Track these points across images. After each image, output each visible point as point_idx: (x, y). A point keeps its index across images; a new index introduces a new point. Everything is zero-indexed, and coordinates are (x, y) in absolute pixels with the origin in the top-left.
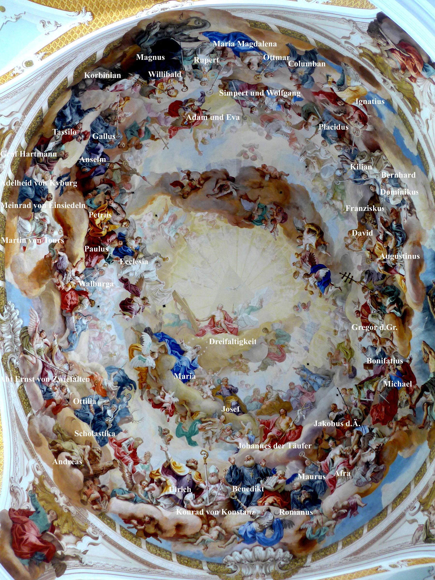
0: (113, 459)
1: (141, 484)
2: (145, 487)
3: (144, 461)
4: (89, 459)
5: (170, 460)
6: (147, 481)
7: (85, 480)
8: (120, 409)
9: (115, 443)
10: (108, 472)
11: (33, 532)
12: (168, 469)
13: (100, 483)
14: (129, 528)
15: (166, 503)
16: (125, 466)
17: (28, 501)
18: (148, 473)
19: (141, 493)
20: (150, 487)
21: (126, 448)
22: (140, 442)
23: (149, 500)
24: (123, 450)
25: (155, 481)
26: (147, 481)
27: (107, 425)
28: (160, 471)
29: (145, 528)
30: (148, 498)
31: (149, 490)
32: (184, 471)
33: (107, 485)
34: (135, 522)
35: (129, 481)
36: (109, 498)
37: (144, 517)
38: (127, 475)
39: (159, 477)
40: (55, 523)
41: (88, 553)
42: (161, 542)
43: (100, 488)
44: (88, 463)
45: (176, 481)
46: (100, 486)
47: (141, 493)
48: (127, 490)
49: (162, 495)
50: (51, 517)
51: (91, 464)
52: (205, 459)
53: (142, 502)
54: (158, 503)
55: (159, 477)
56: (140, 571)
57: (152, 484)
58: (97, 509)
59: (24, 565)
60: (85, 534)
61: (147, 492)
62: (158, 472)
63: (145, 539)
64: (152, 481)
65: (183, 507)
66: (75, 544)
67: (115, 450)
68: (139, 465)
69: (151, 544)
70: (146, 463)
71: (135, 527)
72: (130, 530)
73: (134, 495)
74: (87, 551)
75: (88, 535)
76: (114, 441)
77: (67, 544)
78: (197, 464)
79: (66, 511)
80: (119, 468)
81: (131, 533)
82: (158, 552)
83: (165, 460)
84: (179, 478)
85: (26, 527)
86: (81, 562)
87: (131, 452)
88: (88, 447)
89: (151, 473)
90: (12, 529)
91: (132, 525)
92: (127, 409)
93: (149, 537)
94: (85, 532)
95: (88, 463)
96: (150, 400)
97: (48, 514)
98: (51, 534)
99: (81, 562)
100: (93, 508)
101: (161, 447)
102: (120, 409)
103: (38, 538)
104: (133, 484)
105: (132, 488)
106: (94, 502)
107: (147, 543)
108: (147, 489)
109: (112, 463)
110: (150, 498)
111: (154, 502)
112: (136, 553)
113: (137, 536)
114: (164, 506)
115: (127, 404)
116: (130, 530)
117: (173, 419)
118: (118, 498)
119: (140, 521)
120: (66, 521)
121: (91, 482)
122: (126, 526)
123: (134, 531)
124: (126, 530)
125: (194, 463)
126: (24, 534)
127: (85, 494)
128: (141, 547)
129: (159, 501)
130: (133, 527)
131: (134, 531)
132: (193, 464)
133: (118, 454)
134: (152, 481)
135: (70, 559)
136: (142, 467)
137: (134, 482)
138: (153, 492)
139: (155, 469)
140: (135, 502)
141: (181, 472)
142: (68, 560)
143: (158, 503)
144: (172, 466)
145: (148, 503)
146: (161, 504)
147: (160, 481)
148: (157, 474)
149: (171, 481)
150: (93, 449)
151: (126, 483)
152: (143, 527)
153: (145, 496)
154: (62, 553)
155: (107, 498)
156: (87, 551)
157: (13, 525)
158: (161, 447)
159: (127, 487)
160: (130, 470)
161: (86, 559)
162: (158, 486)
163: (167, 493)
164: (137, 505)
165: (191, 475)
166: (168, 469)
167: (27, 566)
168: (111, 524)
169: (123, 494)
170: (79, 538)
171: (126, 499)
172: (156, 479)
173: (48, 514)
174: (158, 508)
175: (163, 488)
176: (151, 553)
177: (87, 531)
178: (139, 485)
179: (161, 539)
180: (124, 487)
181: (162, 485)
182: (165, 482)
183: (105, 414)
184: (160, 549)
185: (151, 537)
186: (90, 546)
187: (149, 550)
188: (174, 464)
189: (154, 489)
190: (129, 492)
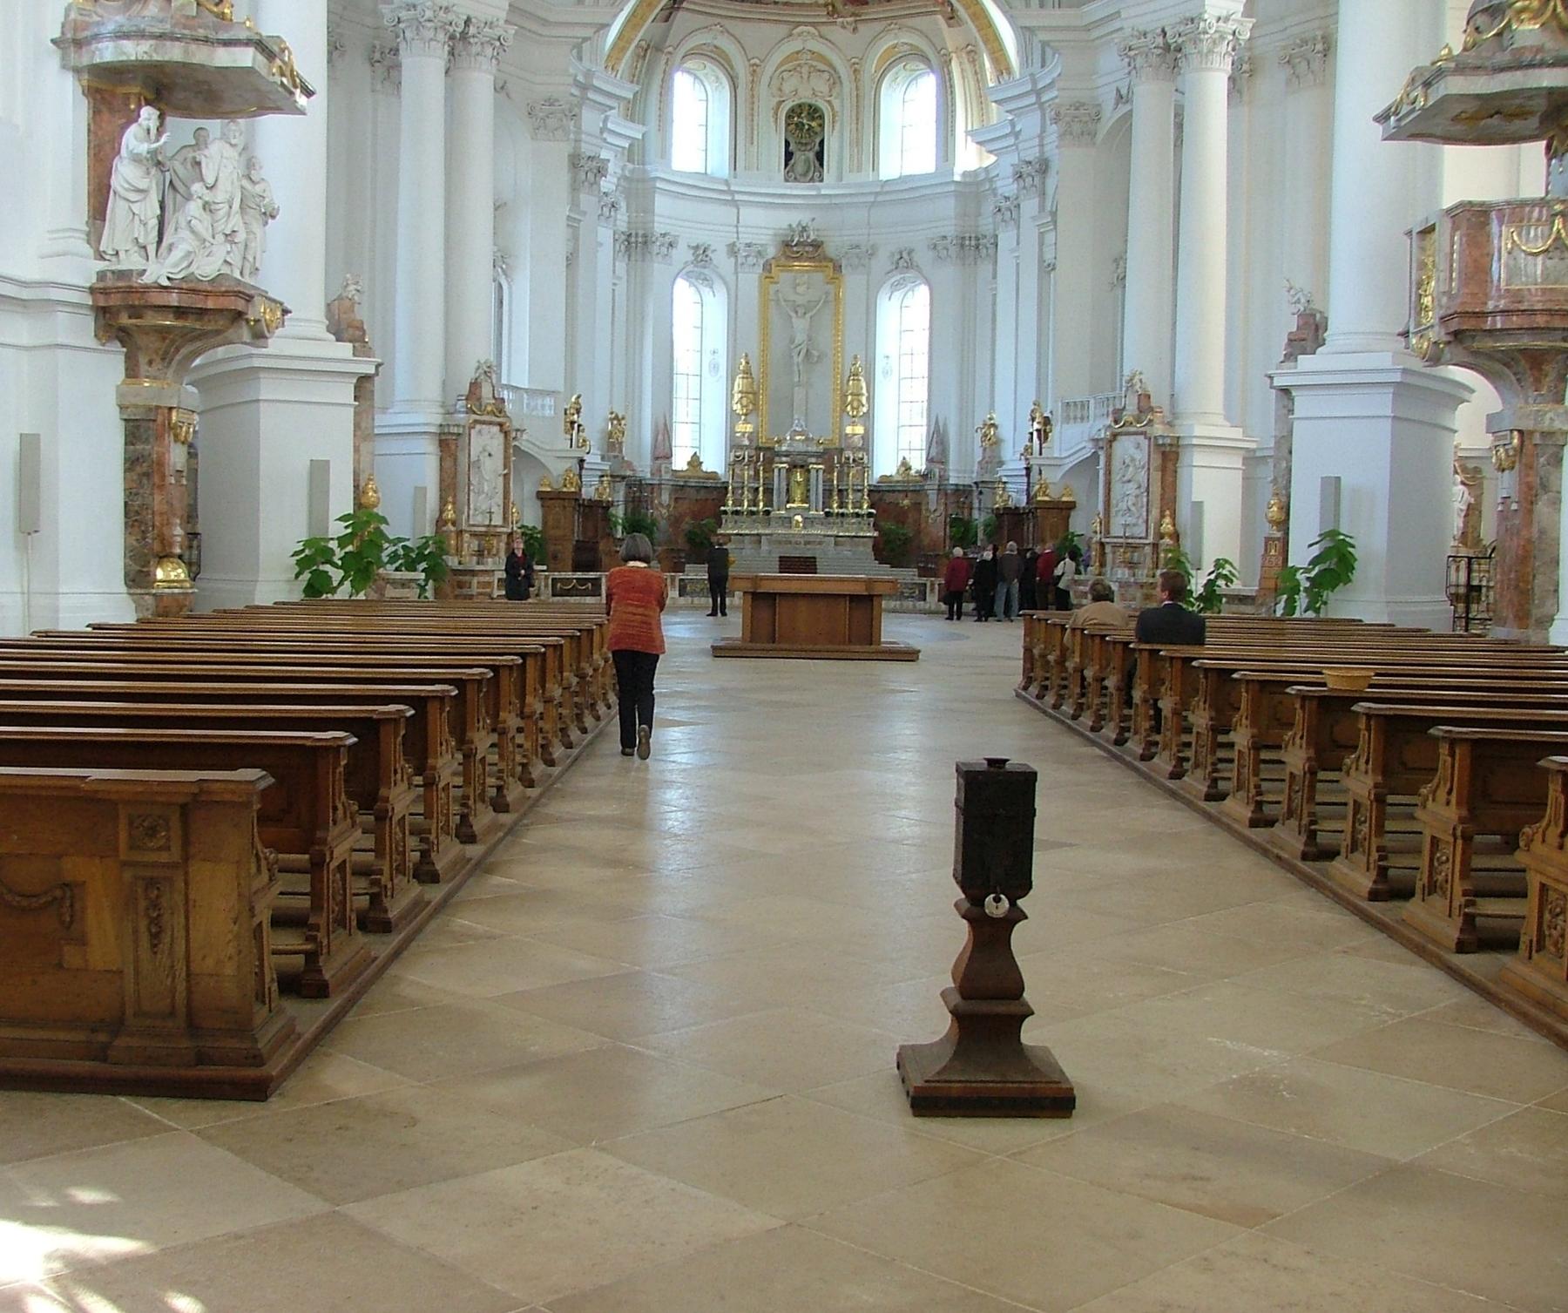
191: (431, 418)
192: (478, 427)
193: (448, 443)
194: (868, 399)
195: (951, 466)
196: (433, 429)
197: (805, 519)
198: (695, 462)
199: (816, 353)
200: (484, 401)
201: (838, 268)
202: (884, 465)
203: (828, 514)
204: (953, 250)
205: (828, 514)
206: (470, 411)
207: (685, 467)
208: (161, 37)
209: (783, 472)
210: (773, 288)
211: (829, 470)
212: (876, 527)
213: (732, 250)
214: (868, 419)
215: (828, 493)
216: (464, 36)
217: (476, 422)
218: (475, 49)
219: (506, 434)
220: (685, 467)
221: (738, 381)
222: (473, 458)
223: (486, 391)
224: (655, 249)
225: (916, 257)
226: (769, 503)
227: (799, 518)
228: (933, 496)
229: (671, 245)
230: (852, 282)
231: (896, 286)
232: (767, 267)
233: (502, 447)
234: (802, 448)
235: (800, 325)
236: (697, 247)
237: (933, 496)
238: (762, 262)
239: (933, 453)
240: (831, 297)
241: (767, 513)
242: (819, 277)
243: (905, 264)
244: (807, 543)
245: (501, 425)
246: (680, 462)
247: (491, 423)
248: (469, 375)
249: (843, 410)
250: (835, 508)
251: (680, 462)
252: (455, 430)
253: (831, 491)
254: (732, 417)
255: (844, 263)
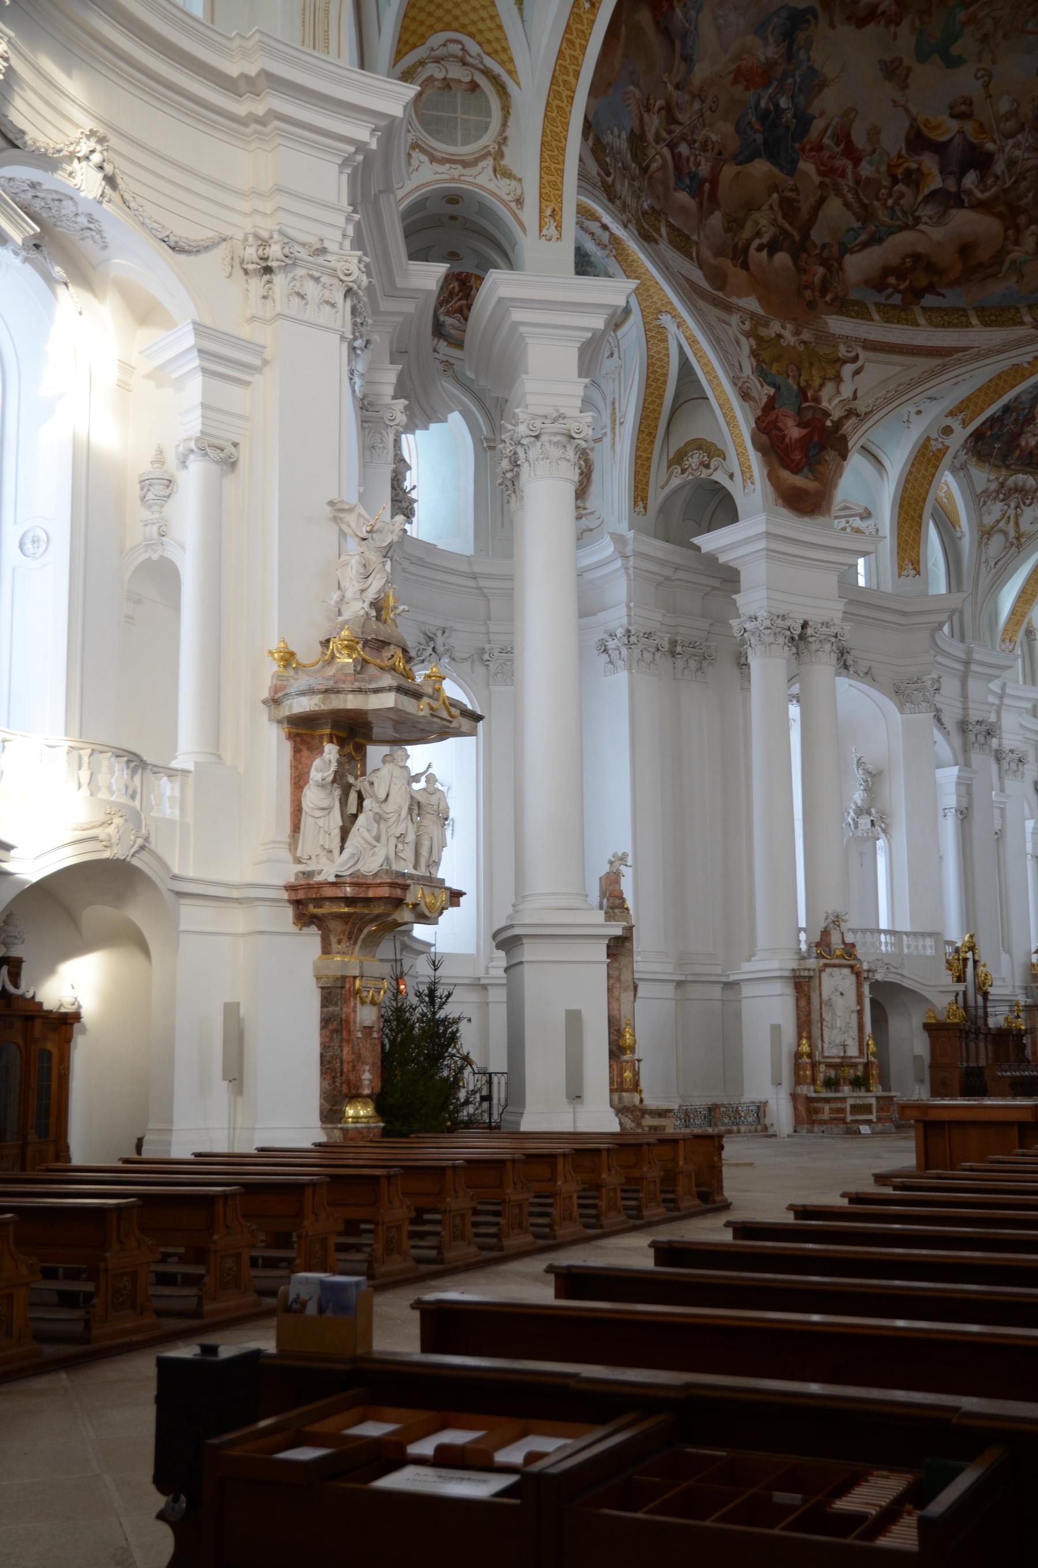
0: (817, 183)
1: (878, 199)
2: (886, 200)
3: (868, 148)
4: (784, 218)
5: (915, 120)
6: (886, 187)
7: (795, 259)
8: (798, 80)
9: (811, 150)
10: (820, 214)
11: (790, 423)
12: (918, 141)
13: (816, 247)
14: (888, 297)
15: (931, 213)
16: (841, 181)
17: (762, 386)
18: (883, 168)
19: (883, 217)
20: (895, 195)
21: (832, 144)
22: (852, 116)
23: (900, 223)
24: (828, 154)
25: (900, 177)
26: (886, 187)
27: (788, 128)
28: (904, 152)
29: (911, 281)
30: (899, 219)
31: (896, 202)
32: (948, 128)
33: (827, 240)
34: (892, 280)
35: (856, 205)
36: (840, 264)
37: (903, 260)
38: (850, 196)
39: (905, 165)
40: (803, 384)
41: (859, 394)
42: (944, 296)
43: (820, 255)
44: (787, 226)
45: (936, 158)
46: (817, 252)
47: (883, 217)
48: (859, 224)
49: (920, 198)
50: (793, 377)
51: (790, 224)
52: (986, 86)
53: (892, 233)
54: (918, 220)
55: (905, 165)
56: (933, 374)
57: (896, 188)
58: (833, 300)
59: (806, 477)
60: (839, 364)
61: (892, 208)
62: (900, 156)
63: (918, 304)
64: (895, 181)
65: (963, 207)
66: (838, 393)
67: (815, 163)
68: (864, 164)
69: (931, 309)
70: (874, 152)
71: (896, 290)
72: (891, 301)
73: (874, 228)
74: (856, 391)
75: (844, 362)
76: (808, 147)
77: (830, 401)
78: (971, 103)
79: (801, 348)
80: (832, 193)
81: (895, 307)
82: (946, 318)
83: (907, 124)
84: (940, 149)
85: (780, 425)
86: (858, 415)
87: (842, 146)
88: (775, 195)
89: (889, 166)
90: (772, 445)
91: (890, 290)
92: (812, 70)
93: (923, 297)
94: (839, 359)
95: (787, 226)
96: (849, 18)
97: (788, 376)
98: (807, 404)
99: (858, 415)
100: (826, 302)
101: (894, 102)
102: (798, 80)
103: (798, 426)
104: (865, 207)
105: (866, 215)
106: (824, 290)
107: (924, 309)
108: (890, 202)
109: (819, 193)
110: (900, 215)
111: (911, 222)
112: (915, 343)
113: (905, 307)
114: (928, 221)
115: (809, 59)
116: (891, 301)
117: (904, 29)
118: (852, 253)
119: (900, 273)
120: (811, 365)
121: (804, 255)
122: (881, 298)
123: (897, 299)
124: (885, 305)
125: (964, 103)
126: (784, 436)
127: (806, 287)
128: (918, 325)
129: (917, 214)
130: (892, 294)
131: (897, 299)
132: (963, 108)
133: (822, 168)
134: (895, 181)
135: (845, 421)
136: (870, 164)
137: (866, 201)
138: (902, 202)
139: (894, 154)
140: (880, 241)
141: (943, 134)
142: (843, 425)
143: (918, 220)
144: (924, 130)
145: (901, 229)
146: (924, 219)
147: (908, 172)
148: (901, 161)
149: (929, 163)
150: (783, 191)
151: (854, 214)
152: (908, 282)
153: (892, 219)
154: (832, 421)
155: (836, 265)
156: (856, 391)
157: (770, 438)
158: (894, 102)
159: (858, 220)
160: (851, 184)
161: (861, 406)
162: (907, 185)
163: (926, 192)
164: (885, 244)
165: (963, 132)
166: (918, 141)
167: (810, 476)
168: (859, 311)
169: (856, 239)
170: (838, 379)
171: (866, 245)
172: (900, 170)
173: (788, 376)
174: (920, 231)
175: (918, 186)
176: (937, 327)
177: (840, 356)
178: (876, 203)
179: (942, 291)
180: (856, 224)
181: (914, 178)
182: (919, 169)
183: (779, 111)
184: (946, 311)
185: (927, 296)
186: (857, 377)
187: (931, 323)
188: (927, 123)
189: (902, 195)
190: (864, 228)
191: (782, 963)
192: (829, 970)
193: (802, 985)
196: (787, 974)
200: (833, 947)
206: (820, 956)
208: (327, 691)
216: (802, 637)
217: (826, 965)
218: (814, 647)
219: (858, 974)
222: (825, 997)
223: (835, 939)
233: (854, 987)
245: (852, 967)
247: (841, 966)
248: (822, 925)
252: (806, 973)
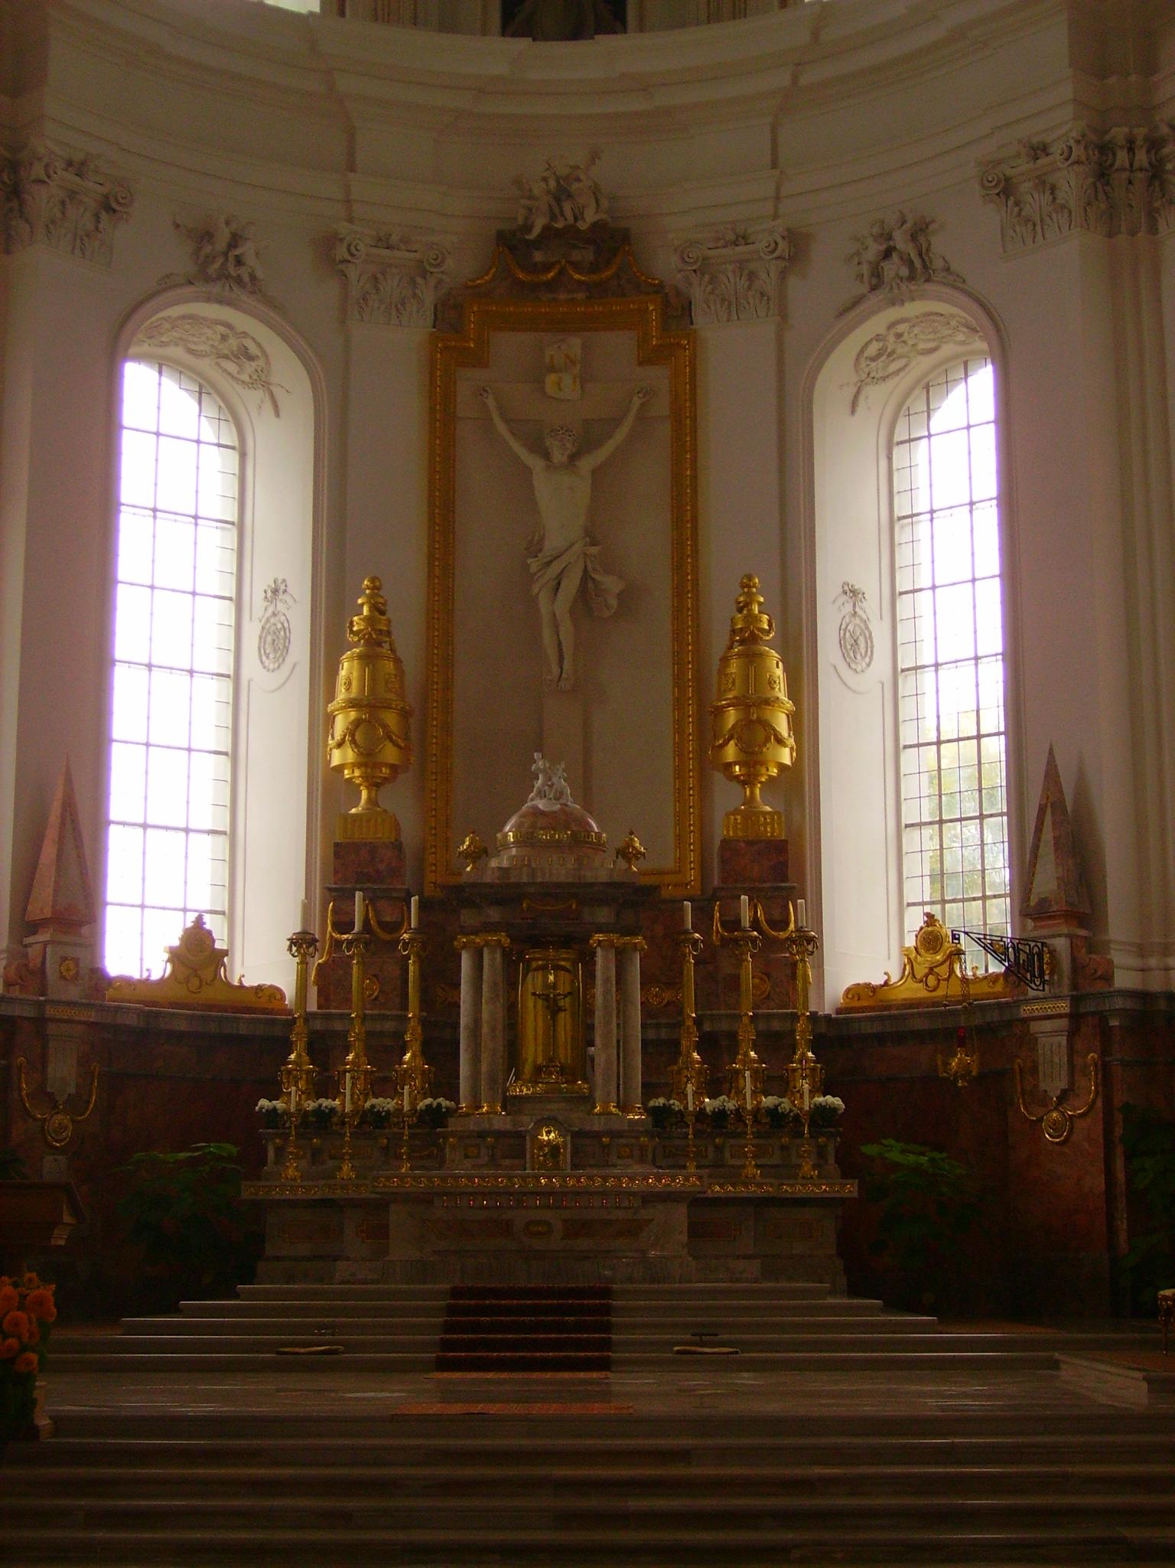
194: (795, 721)
195: (1119, 924)
197: (579, 1137)
198: (198, 953)
199: (612, 584)
201: (678, 311)
202: (862, 949)
203: (660, 1116)
204: (1071, 183)
205: (660, 1116)
207: (158, 968)
209: (491, 961)
210: (467, 381)
211: (663, 973)
212: (849, 1167)
213: (329, 252)
214: (800, 786)
215: (661, 1052)
220: (158, 968)
221: (347, 668)
224: (42, 200)
225: (940, 245)
226: (444, 1081)
227: (548, 1136)
228: (1051, 1039)
229: (108, 206)
230: (731, 352)
231: (877, 363)
232: (449, 316)
234: (559, 869)
235: (560, 503)
236: (206, 236)
237: (1051, 1039)
238: (429, 298)
239: (1047, 881)
240: (661, 407)
241: (435, 1118)
242: (617, 347)
243: (903, 259)
244: (577, 1229)
246: (135, 946)
249: (708, 763)
250: (693, 1099)
251: (135, 946)
253: (673, 1048)
254: (326, 790)
255: (698, 293)
